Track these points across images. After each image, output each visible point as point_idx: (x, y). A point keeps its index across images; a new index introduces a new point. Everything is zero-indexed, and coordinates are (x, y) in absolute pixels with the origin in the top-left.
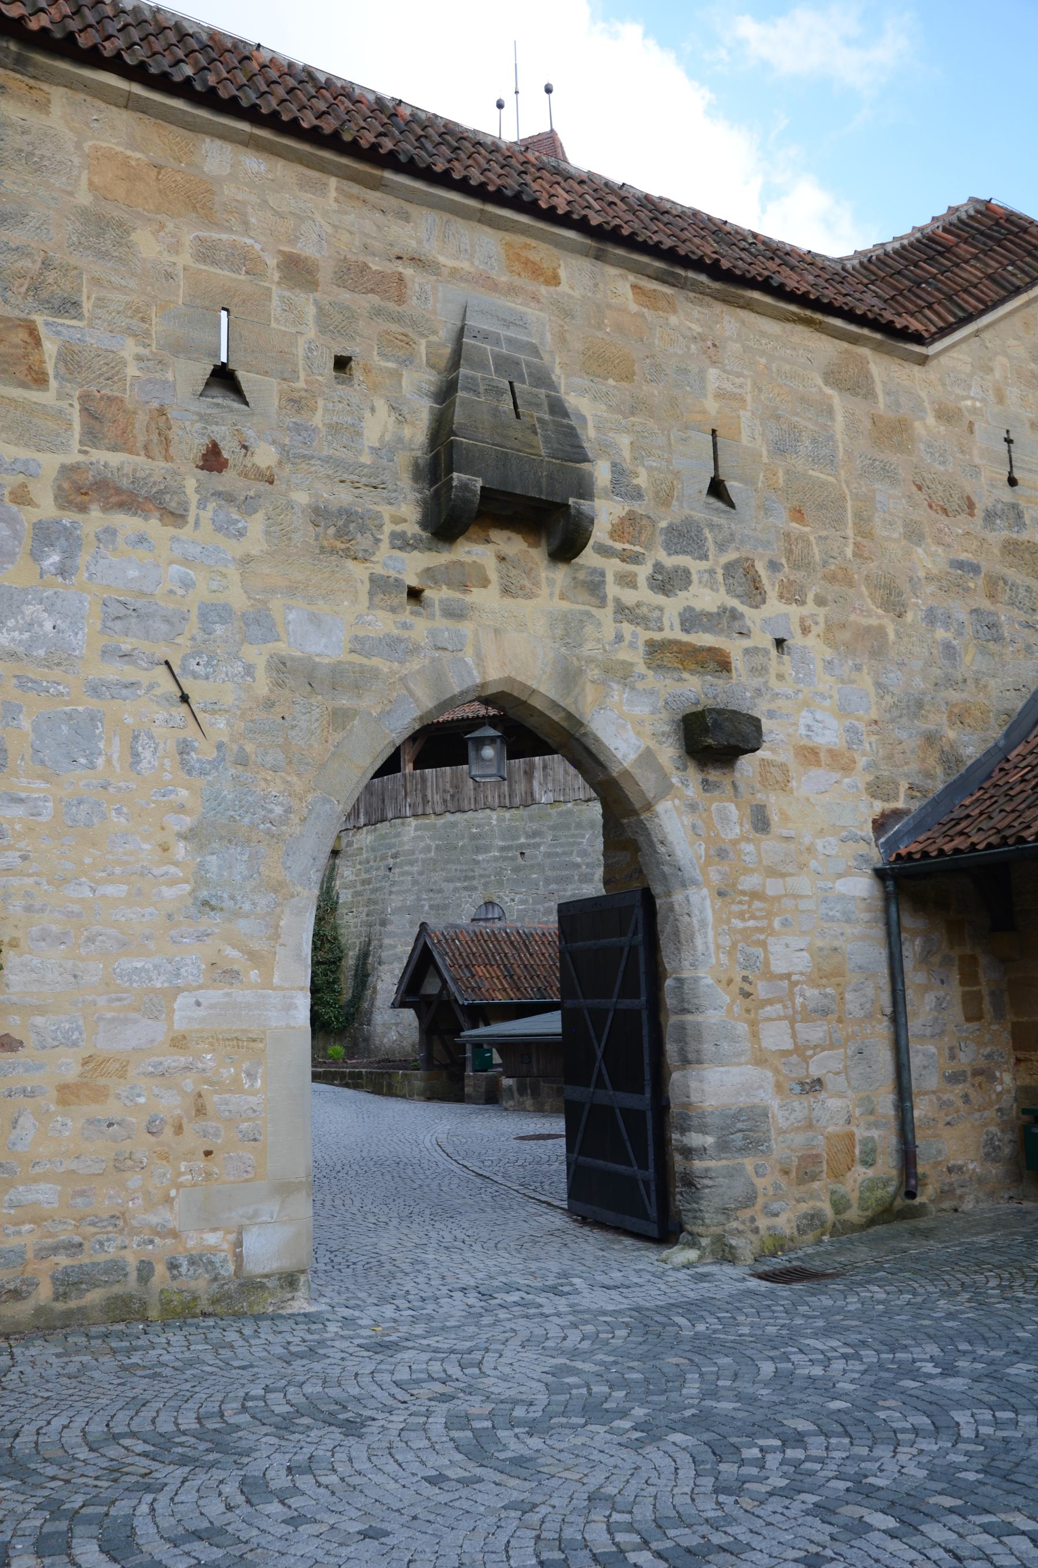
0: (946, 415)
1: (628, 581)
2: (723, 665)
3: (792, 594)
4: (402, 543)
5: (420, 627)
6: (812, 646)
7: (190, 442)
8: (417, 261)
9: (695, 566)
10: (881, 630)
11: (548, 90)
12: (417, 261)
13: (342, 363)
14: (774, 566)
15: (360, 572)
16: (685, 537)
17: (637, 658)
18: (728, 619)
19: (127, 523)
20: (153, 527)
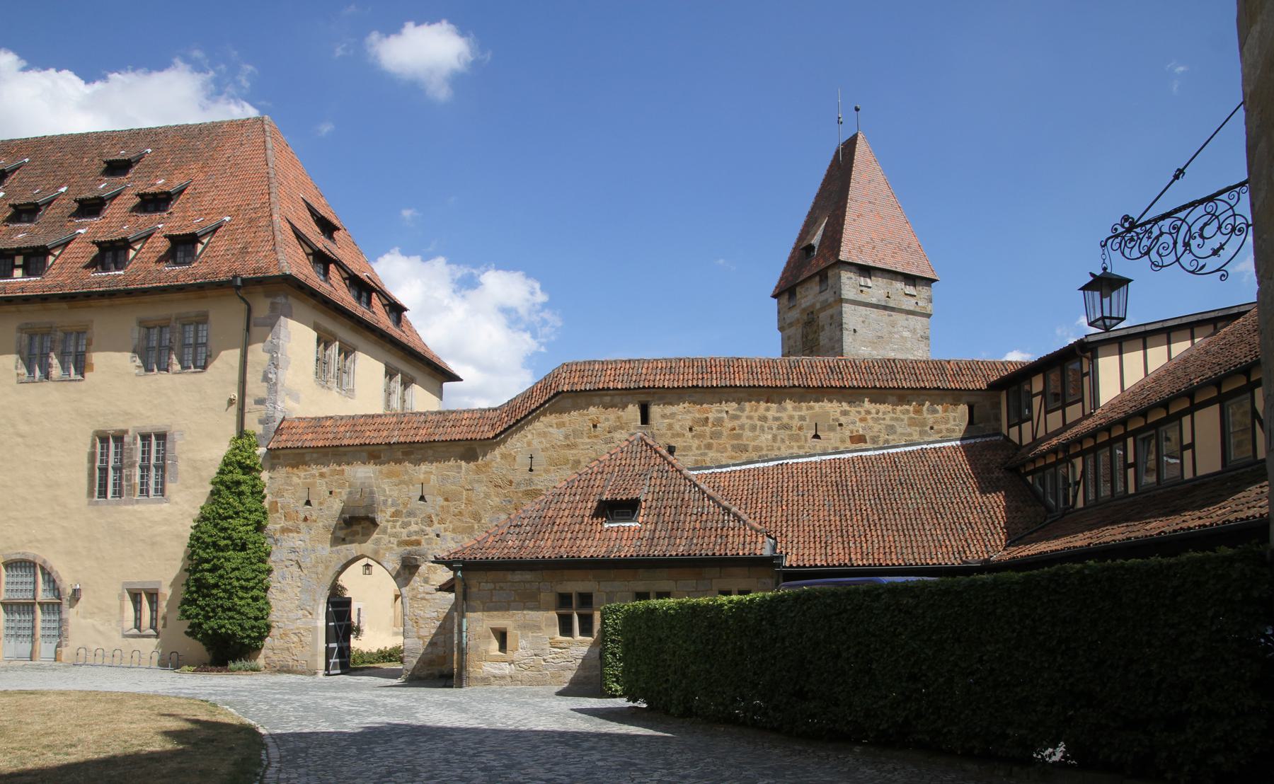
2: (418, 543)
3: (441, 522)
9: (413, 520)
10: (472, 527)
16: (411, 514)
17: (395, 546)
20: (295, 535)
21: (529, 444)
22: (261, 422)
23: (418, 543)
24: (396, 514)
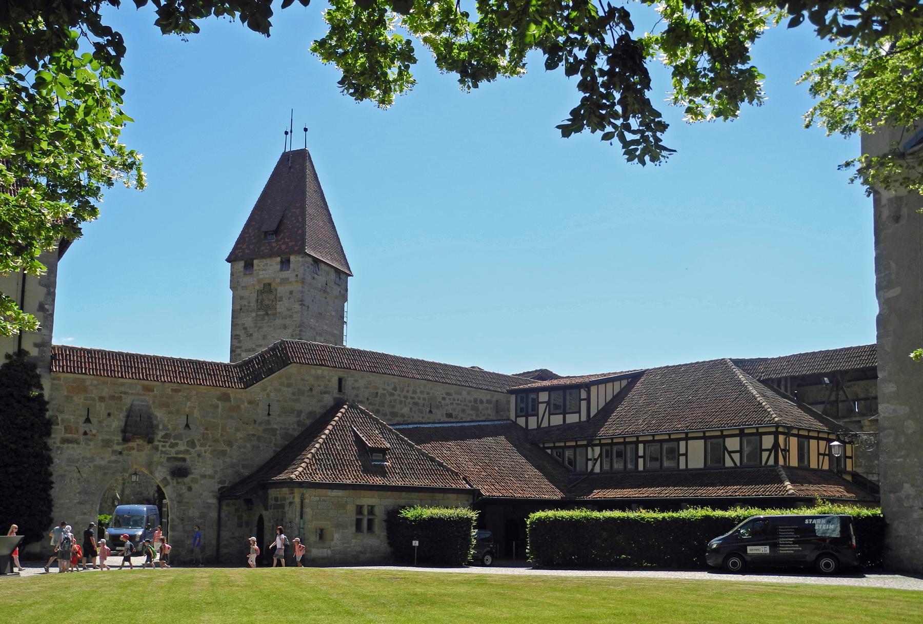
0: (250, 402)
1: (163, 446)
3: (202, 445)
4: (118, 444)
5: (120, 458)
6: (208, 455)
7: (82, 430)
8: (125, 393)
11: (306, 130)
12: (125, 393)
13: (109, 415)
14: (199, 440)
15: (110, 449)
17: (164, 460)
18: (187, 452)
19: (70, 445)
20: (75, 446)
21: (268, 395)
22: (36, 345)
23: (184, 460)
24: (167, 436)
